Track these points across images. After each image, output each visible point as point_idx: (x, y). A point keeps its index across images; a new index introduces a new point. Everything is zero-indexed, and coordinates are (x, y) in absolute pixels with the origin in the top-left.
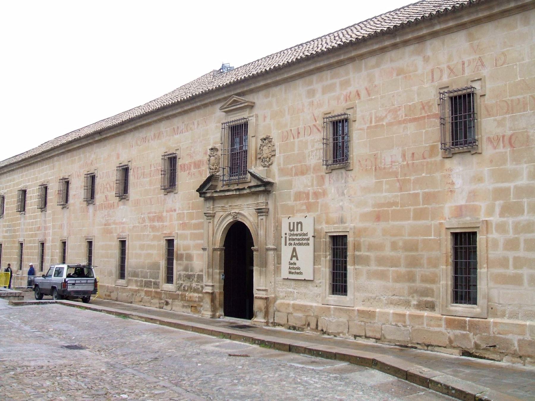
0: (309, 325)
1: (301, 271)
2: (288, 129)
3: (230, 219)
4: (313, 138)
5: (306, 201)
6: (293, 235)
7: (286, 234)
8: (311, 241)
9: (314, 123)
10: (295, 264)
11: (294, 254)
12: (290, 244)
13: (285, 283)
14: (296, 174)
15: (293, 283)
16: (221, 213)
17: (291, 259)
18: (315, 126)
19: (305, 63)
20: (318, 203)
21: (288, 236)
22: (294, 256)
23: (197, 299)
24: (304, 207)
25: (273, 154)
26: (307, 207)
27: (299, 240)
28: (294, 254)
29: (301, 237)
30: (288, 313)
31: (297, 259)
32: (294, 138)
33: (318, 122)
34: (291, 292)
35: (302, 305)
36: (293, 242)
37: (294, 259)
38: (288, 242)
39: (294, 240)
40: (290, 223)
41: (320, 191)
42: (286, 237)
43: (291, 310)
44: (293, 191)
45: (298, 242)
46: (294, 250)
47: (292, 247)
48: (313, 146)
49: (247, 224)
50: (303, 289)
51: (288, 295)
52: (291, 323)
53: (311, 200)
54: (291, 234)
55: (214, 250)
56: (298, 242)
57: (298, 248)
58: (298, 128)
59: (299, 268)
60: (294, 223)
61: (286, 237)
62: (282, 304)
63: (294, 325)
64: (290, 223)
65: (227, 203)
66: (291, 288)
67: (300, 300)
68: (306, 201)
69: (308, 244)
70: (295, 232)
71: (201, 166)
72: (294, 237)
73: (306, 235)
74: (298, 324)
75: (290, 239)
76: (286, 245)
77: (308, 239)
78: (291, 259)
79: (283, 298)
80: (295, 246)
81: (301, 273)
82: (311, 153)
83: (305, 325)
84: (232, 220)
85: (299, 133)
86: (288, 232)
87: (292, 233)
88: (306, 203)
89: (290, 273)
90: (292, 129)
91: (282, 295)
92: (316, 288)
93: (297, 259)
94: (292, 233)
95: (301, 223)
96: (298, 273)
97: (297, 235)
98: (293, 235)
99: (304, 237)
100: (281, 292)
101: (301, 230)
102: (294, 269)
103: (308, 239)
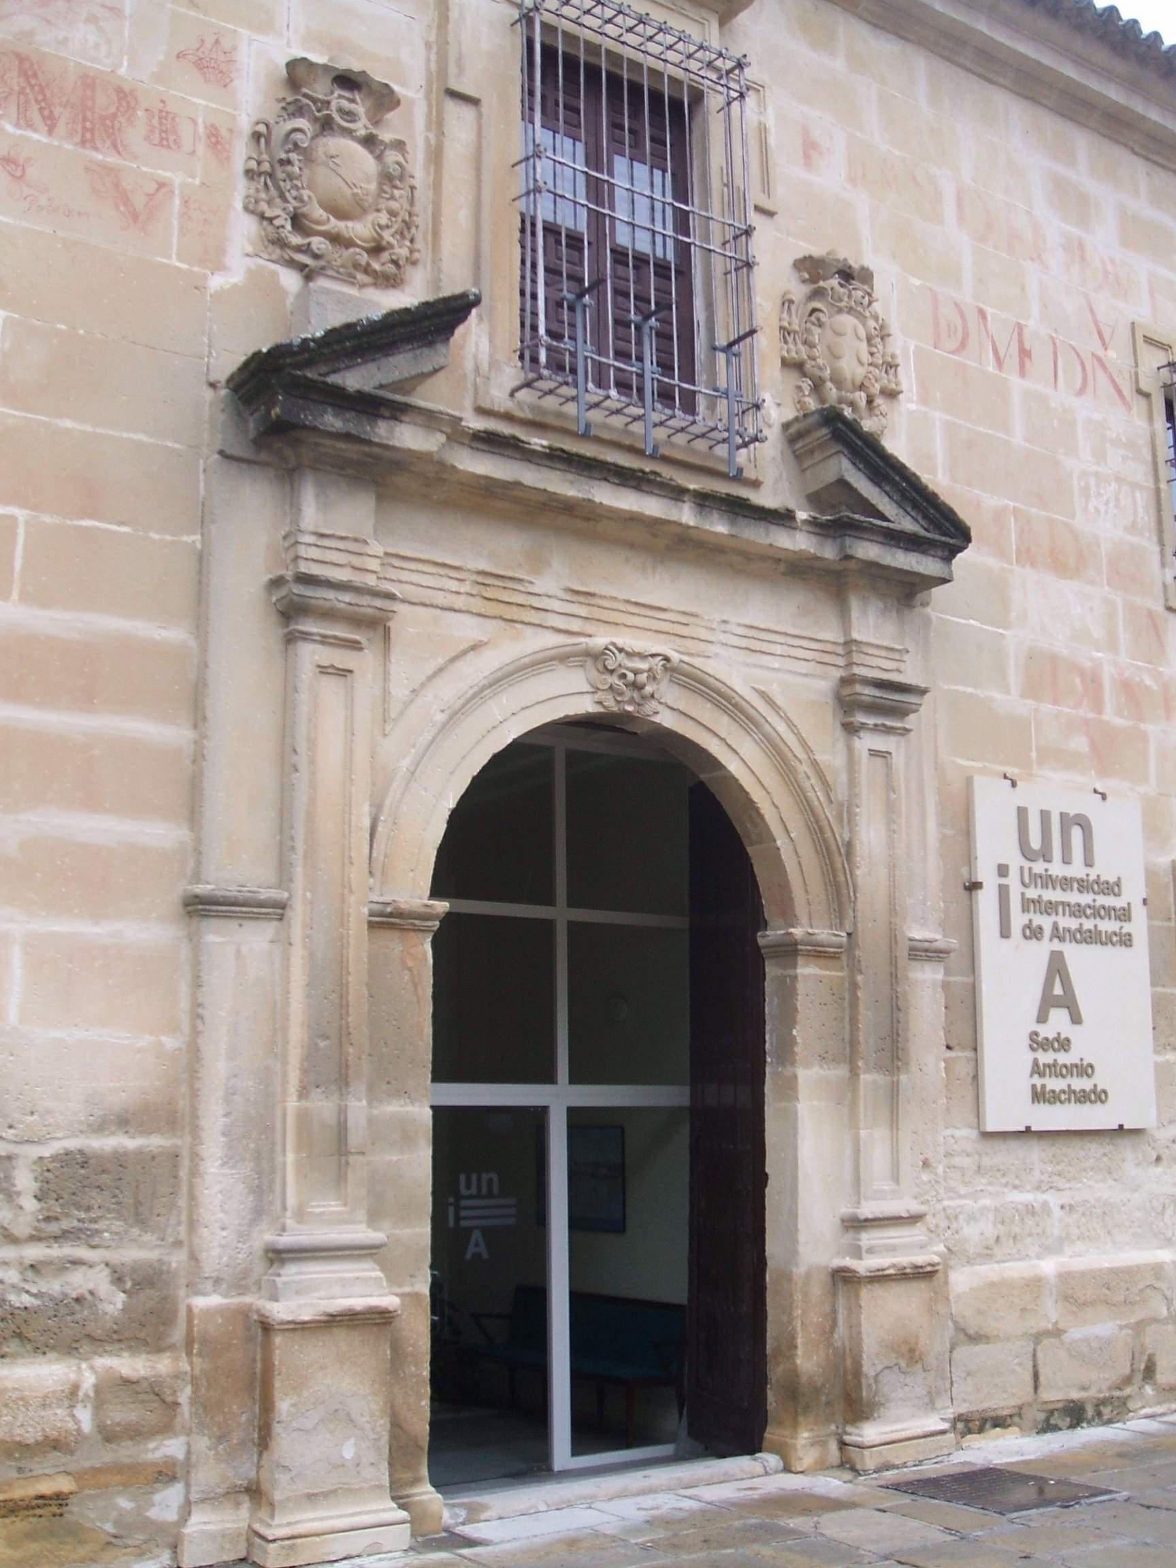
0: (1149, 1372)
1: (1100, 1080)
2: (966, 296)
3: (570, 695)
4: (1097, 416)
5: (1085, 712)
6: (1048, 881)
7: (1003, 871)
8: (1139, 926)
9: (1100, 352)
10: (1064, 1044)
11: (1058, 990)
12: (1033, 933)
13: (986, 1161)
14: (1027, 556)
15: (1035, 1153)
16: (468, 629)
17: (1042, 1018)
18: (1100, 360)
19: (1101, 55)
20: (1144, 737)
21: (1013, 881)
22: (1058, 1003)
23: (85, 1417)
24: (1079, 743)
25: (886, 381)
26: (1093, 744)
27: (1078, 911)
28: (1058, 990)
29: (1085, 899)
30: (1038, 1337)
31: (1076, 1019)
32: (999, 363)
33: (1112, 354)
34: (1031, 1211)
35: (1114, 1272)
36: (1046, 922)
37: (1058, 1021)
38: (1018, 920)
39: (1050, 908)
40: (1022, 813)
41: (1148, 682)
42: (1003, 891)
43: (1051, 1312)
44: (1015, 640)
45: (1072, 923)
46: (1057, 967)
47: (1045, 947)
48: (1100, 455)
49: (741, 760)
50: (1092, 1183)
51: (1017, 1228)
52: (1053, 1394)
53: (1109, 715)
54: (1035, 877)
55: (388, 921)
56: (1072, 923)
57: (1075, 955)
58: (1020, 328)
59: (1084, 1070)
60: (1045, 816)
61: (1003, 891)
62: (997, 1288)
63: (1075, 1395)
64: (1022, 813)
65: (538, 564)
66: (1028, 1185)
67: (1079, 1246)
68: (1085, 712)
69: (1126, 941)
70: (1057, 869)
71: (135, 134)
72: (1051, 895)
73: (1112, 888)
74: (1093, 1382)
75: (1027, 904)
76: (1005, 933)
77: (1124, 915)
78: (1042, 1018)
79: (987, 1254)
80: (1056, 945)
81: (1098, 1096)
82: (1092, 481)
83: (1128, 1380)
84: (585, 706)
85: (1025, 353)
86: (1015, 861)
87: (1039, 867)
88: (1087, 722)
89: (1039, 1096)
90: (989, 311)
91: (974, 1233)
92: (1159, 1170)
93: (1076, 1019)
94: (1039, 867)
95: (1083, 823)
96: (1083, 1097)
97: (1066, 883)
98: (1048, 881)
99: (1102, 900)
100: (972, 1218)
101: (1089, 863)
102: (1058, 1072)
103: (1124, 915)
